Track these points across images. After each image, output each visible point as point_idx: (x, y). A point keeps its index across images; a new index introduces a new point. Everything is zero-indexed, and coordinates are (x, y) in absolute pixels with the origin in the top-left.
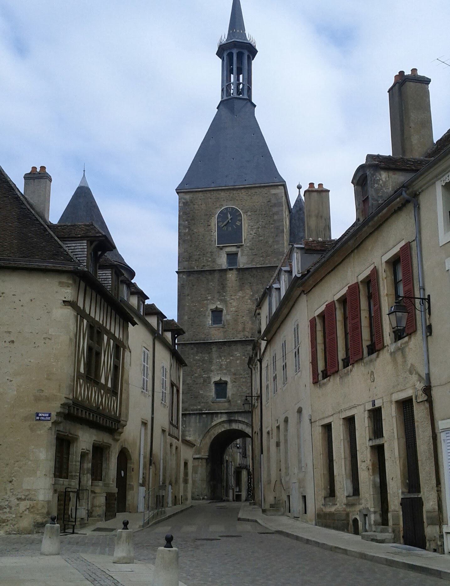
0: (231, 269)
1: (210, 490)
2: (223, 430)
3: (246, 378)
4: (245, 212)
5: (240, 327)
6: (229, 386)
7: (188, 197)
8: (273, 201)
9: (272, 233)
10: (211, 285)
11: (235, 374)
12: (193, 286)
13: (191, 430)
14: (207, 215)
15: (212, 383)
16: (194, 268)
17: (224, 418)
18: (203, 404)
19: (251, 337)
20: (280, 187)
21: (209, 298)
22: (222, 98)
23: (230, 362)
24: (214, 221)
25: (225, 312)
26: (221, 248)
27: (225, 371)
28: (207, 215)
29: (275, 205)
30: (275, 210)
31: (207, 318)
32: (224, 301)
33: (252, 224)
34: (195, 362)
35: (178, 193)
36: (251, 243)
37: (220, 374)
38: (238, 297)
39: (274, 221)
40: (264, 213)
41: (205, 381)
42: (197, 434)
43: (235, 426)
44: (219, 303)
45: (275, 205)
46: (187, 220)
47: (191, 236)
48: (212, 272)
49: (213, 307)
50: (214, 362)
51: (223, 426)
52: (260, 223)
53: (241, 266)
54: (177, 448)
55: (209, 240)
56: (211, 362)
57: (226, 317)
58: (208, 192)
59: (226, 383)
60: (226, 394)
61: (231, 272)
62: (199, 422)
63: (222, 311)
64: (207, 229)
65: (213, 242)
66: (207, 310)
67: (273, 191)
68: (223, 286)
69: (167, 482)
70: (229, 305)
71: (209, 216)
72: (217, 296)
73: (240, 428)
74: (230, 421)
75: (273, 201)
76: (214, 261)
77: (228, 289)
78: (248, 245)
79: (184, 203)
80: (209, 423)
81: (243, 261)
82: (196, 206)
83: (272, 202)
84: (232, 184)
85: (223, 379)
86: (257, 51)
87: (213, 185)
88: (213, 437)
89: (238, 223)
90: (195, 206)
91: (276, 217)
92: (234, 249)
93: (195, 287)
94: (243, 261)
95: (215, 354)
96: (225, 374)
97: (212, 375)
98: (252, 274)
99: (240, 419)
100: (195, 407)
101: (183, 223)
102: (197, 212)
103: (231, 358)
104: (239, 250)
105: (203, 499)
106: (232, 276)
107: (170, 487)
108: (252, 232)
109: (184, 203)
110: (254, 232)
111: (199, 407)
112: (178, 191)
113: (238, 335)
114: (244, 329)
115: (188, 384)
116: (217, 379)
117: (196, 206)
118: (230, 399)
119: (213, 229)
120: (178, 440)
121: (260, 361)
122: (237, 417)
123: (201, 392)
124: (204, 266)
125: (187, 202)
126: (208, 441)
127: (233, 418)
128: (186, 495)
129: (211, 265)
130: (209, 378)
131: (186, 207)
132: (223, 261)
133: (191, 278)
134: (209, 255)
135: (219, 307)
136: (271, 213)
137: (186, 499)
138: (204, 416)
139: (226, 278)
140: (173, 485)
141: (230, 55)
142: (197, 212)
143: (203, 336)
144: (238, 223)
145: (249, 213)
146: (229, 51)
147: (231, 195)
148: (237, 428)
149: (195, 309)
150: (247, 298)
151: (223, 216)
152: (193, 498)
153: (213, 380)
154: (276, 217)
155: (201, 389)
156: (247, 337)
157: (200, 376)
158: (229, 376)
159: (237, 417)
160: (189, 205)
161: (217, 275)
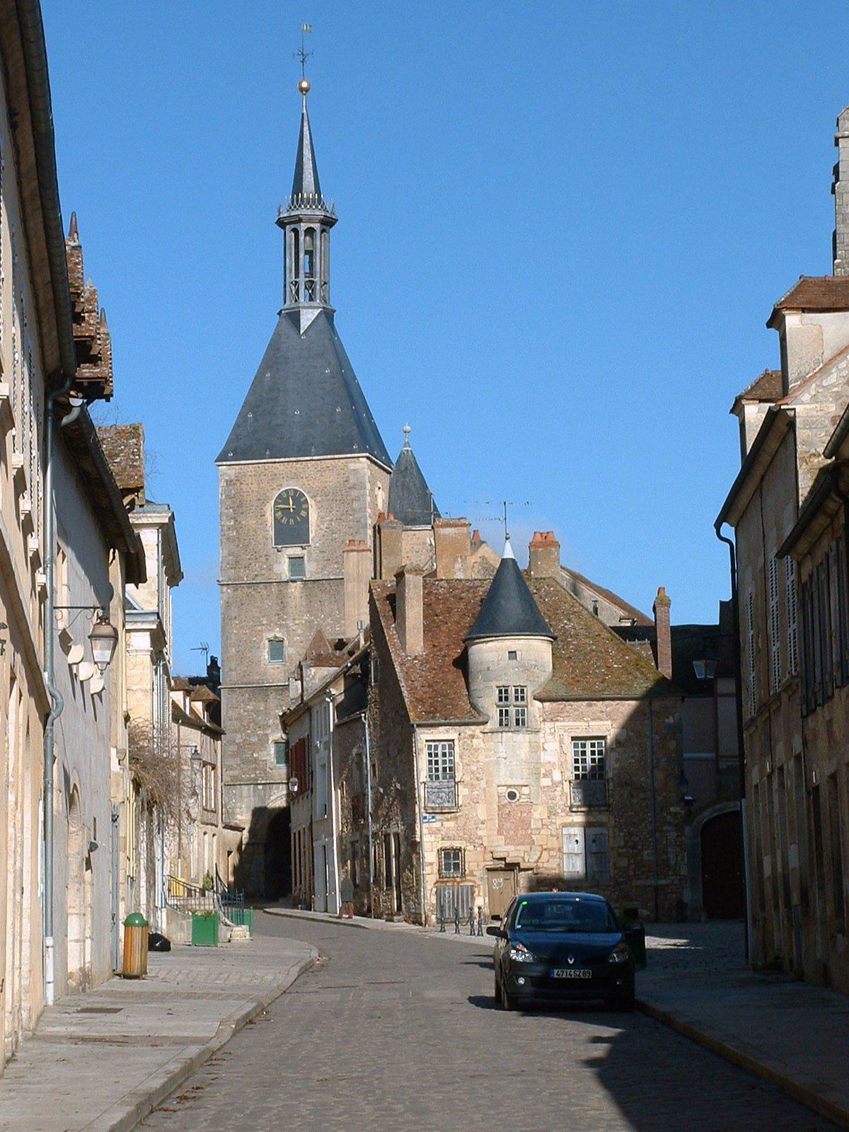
0: (293, 581)
4: (314, 497)
8: (352, 480)
12: (242, 604)
13: (243, 806)
14: (259, 500)
16: (243, 580)
21: (264, 622)
25: (286, 642)
28: (259, 500)
29: (353, 487)
30: (354, 493)
31: (262, 652)
33: (322, 514)
34: (246, 713)
36: (321, 542)
39: (353, 510)
40: (339, 498)
45: (353, 487)
46: (231, 508)
49: (271, 636)
52: (334, 512)
53: (308, 577)
61: (295, 584)
62: (254, 796)
63: (282, 641)
64: (260, 521)
66: (261, 640)
67: (352, 466)
68: (283, 605)
70: (292, 633)
71: (263, 501)
75: (352, 480)
76: (270, 569)
77: (290, 610)
78: (317, 545)
79: (227, 481)
81: (311, 570)
82: (244, 487)
83: (351, 481)
89: (303, 513)
90: (242, 486)
94: (311, 570)
97: (268, 731)
98: (323, 588)
101: (226, 511)
102: (245, 495)
104: (305, 551)
106: (295, 589)
108: (322, 526)
109: (227, 481)
117: (244, 487)
120: (216, 826)
124: (256, 575)
125: (231, 481)
132: (283, 569)
134: (263, 560)
136: (349, 498)
138: (260, 787)
142: (245, 495)
144: (303, 513)
145: (319, 499)
151: (282, 499)
154: (355, 505)
160: (235, 484)
161: (274, 588)
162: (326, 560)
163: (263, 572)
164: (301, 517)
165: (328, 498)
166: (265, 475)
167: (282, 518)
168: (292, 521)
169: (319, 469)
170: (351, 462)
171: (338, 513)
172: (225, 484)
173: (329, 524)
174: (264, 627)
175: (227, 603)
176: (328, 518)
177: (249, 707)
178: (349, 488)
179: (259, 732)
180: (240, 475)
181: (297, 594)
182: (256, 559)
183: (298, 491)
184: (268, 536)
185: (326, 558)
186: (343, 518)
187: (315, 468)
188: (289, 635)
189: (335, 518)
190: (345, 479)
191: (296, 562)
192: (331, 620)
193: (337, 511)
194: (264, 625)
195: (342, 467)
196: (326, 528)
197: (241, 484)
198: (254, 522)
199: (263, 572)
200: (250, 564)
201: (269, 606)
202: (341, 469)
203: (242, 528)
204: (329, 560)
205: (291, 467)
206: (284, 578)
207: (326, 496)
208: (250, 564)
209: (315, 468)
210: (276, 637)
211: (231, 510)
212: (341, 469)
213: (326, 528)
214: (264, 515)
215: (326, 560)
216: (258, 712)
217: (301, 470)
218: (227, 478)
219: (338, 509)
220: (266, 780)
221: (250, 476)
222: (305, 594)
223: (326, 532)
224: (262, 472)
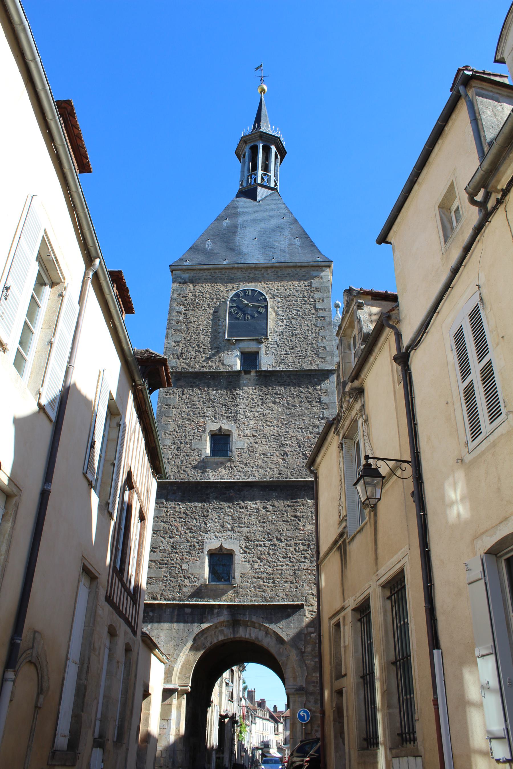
2: (221, 638)
13: (162, 635)
22: (252, 131)
25: (234, 436)
30: (317, 295)
35: (172, 272)
43: (243, 633)
44: (224, 421)
51: (222, 632)
54: (128, 650)
57: (238, 442)
59: (229, 555)
65: (221, 334)
69: (87, 739)
73: (253, 636)
81: (267, 362)
85: (226, 546)
86: (286, 153)
94: (267, 362)
98: (281, 381)
112: (173, 268)
119: (223, 316)
120: (135, 633)
121: (403, 359)
130: (201, 543)
135: (224, 427)
141: (254, 150)
146: (252, 144)
147: (252, 276)
148: (247, 636)
153: (208, 547)
164: (260, 313)
166: (221, 279)
167: (237, 313)
168: (248, 317)
169: (279, 275)
170: (314, 270)
180: (194, 279)
183: (256, 291)
184: (220, 330)
187: (275, 274)
191: (250, 359)
195: (304, 274)
202: (303, 276)
205: (250, 273)
209: (275, 274)
212: (303, 276)
217: (260, 276)
218: (181, 280)
221: (205, 279)
224: (218, 277)
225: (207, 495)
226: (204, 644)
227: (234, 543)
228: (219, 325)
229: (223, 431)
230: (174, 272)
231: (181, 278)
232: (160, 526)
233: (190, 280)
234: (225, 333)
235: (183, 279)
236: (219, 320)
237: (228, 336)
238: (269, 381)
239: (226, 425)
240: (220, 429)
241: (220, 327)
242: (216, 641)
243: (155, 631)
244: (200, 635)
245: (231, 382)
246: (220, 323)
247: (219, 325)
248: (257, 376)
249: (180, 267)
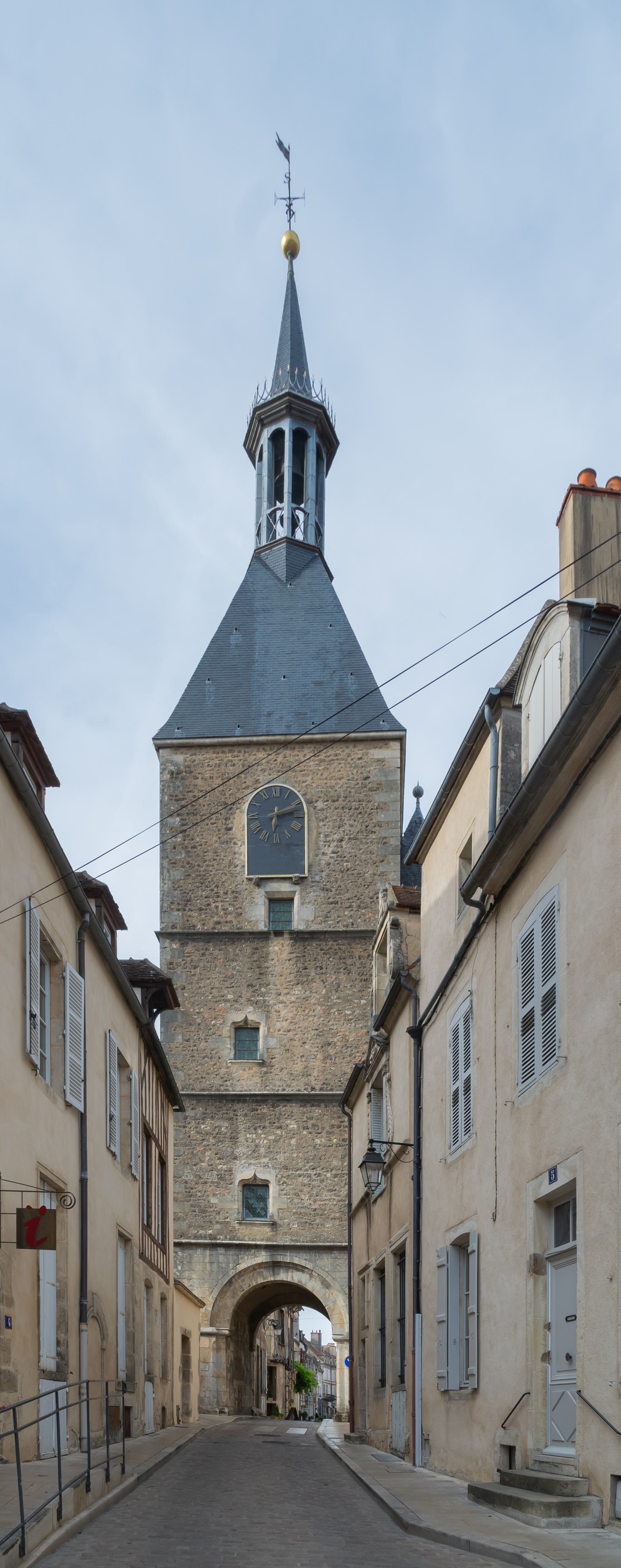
0: (279, 934)
1: (232, 1397)
2: (261, 1281)
3: (309, 1176)
5: (299, 1067)
6: (273, 1190)
7: (179, 758)
9: (371, 853)
10: (234, 969)
11: (286, 1168)
13: (194, 1276)
15: (237, 1183)
17: (263, 1257)
18: (218, 1227)
19: (321, 1089)
20: (392, 744)
21: (230, 997)
23: (276, 1141)
24: (241, 820)
26: (259, 883)
27: (266, 1160)
29: (378, 788)
30: (379, 798)
32: (264, 1007)
35: (158, 748)
37: (254, 1164)
38: (293, 999)
41: (221, 1178)
42: (206, 1285)
44: (251, 1009)
47: (188, 852)
48: (236, 936)
49: (238, 1017)
50: (241, 1139)
52: (347, 827)
55: (231, 864)
56: (234, 1139)
58: (226, 749)
60: (265, 1209)
65: (238, 869)
68: (261, 970)
70: (274, 1015)
72: (246, 993)
74: (275, 1265)
79: (172, 773)
80: (231, 1265)
84: (283, 730)
85: (260, 1176)
87: (238, 731)
88: (240, 1294)
91: (381, 817)
92: (285, 888)
93: (198, 970)
95: (242, 1124)
96: (266, 1166)
99: (296, 1261)
100: (201, 1232)
103: (279, 1132)
105: (221, 1412)
107: (149, 1385)
109: (172, 773)
110: (331, 849)
111: (210, 1232)
113: (294, 1083)
114: (306, 1074)
115: (186, 1182)
116: (247, 1174)
117: (199, 782)
118: (276, 1218)
119: (239, 836)
122: (287, 1258)
123: (213, 1200)
124: (218, 923)
125: (179, 773)
126: (231, 1302)
127: (280, 1259)
128: (186, 1405)
129: (235, 923)
131: (178, 783)
132: (258, 916)
133: (189, 948)
135: (251, 1017)
136: (370, 805)
137: (188, 1413)
139: (268, 954)
140: (157, 1380)
143: (217, 1082)
149: (199, 1021)
150: (313, 1001)
152: (201, 1411)
154: (381, 817)
155: (214, 1195)
156: (313, 1089)
157: (212, 1168)
158: (274, 1172)
159: (287, 1258)
162: (332, 903)
163: (229, 918)
165: (336, 804)
171: (352, 829)
172: (169, 776)
173: (337, 846)
174: (228, 1004)
175: (171, 963)
176: (335, 836)
177: (203, 1126)
178: (371, 790)
179: (220, 1167)
181: (285, 955)
182: (218, 897)
185: (331, 900)
186: (360, 836)
188: (268, 1017)
189: (346, 837)
190: (365, 775)
192: (338, 998)
193: (352, 826)
194: (227, 1001)
196: (333, 852)
197: (196, 778)
198: (215, 838)
199: (229, 918)
200: (209, 905)
201: (238, 971)
203: (194, 847)
204: (337, 903)
206: (262, 927)
207: (334, 801)
208: (209, 905)
210: (246, 1020)
211: (178, 819)
213: (333, 852)
214: (230, 829)
215: (332, 903)
216: (218, 1135)
218: (172, 768)
219: (352, 822)
220: (230, 1239)
222: (295, 955)
223: (331, 857)
224: (229, 761)
225: (235, 1111)
226: (241, 1287)
227: (270, 1173)
228: (235, 853)
229: (250, 1022)
230: (161, 751)
231: (172, 762)
232: (179, 1150)
233: (185, 767)
234: (244, 866)
235: (176, 765)
236: (235, 844)
237: (248, 874)
238: (309, 948)
239: (253, 1015)
240: (246, 1020)
241: (237, 856)
242: (254, 1284)
243: (187, 1273)
244: (237, 1277)
245: (257, 949)
246: (236, 849)
247: (235, 853)
248: (291, 939)
249: (169, 741)
